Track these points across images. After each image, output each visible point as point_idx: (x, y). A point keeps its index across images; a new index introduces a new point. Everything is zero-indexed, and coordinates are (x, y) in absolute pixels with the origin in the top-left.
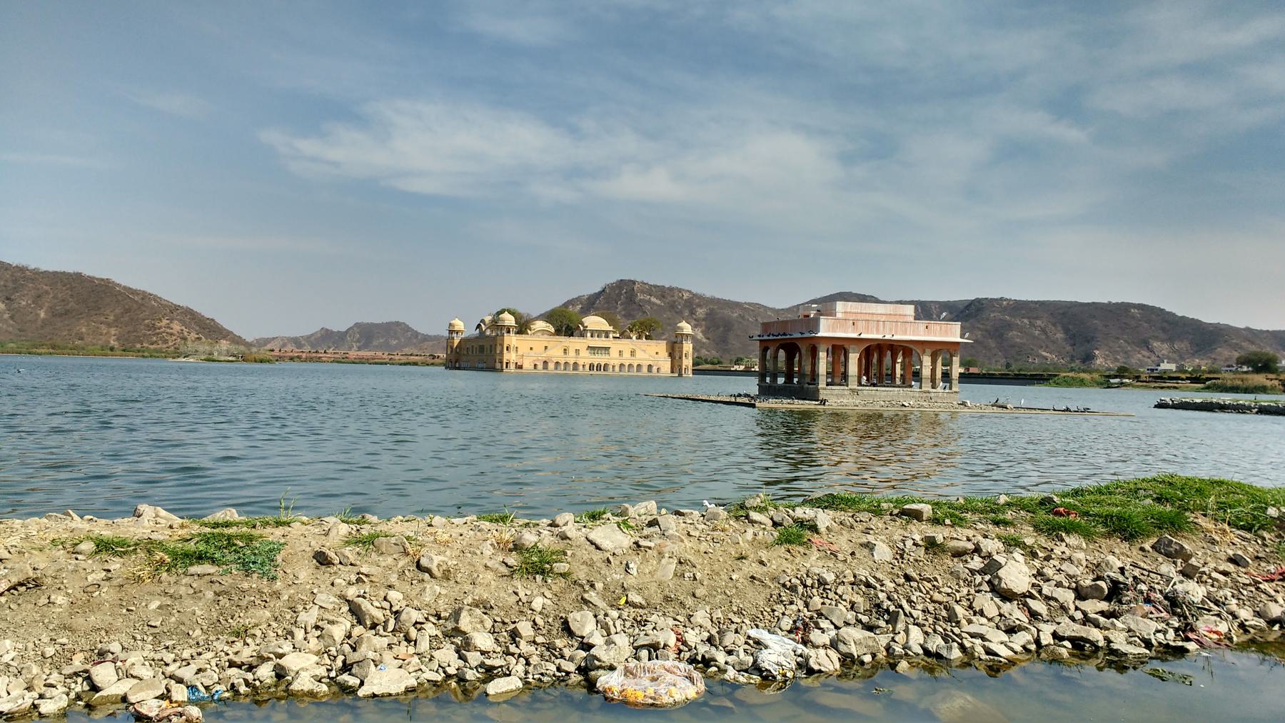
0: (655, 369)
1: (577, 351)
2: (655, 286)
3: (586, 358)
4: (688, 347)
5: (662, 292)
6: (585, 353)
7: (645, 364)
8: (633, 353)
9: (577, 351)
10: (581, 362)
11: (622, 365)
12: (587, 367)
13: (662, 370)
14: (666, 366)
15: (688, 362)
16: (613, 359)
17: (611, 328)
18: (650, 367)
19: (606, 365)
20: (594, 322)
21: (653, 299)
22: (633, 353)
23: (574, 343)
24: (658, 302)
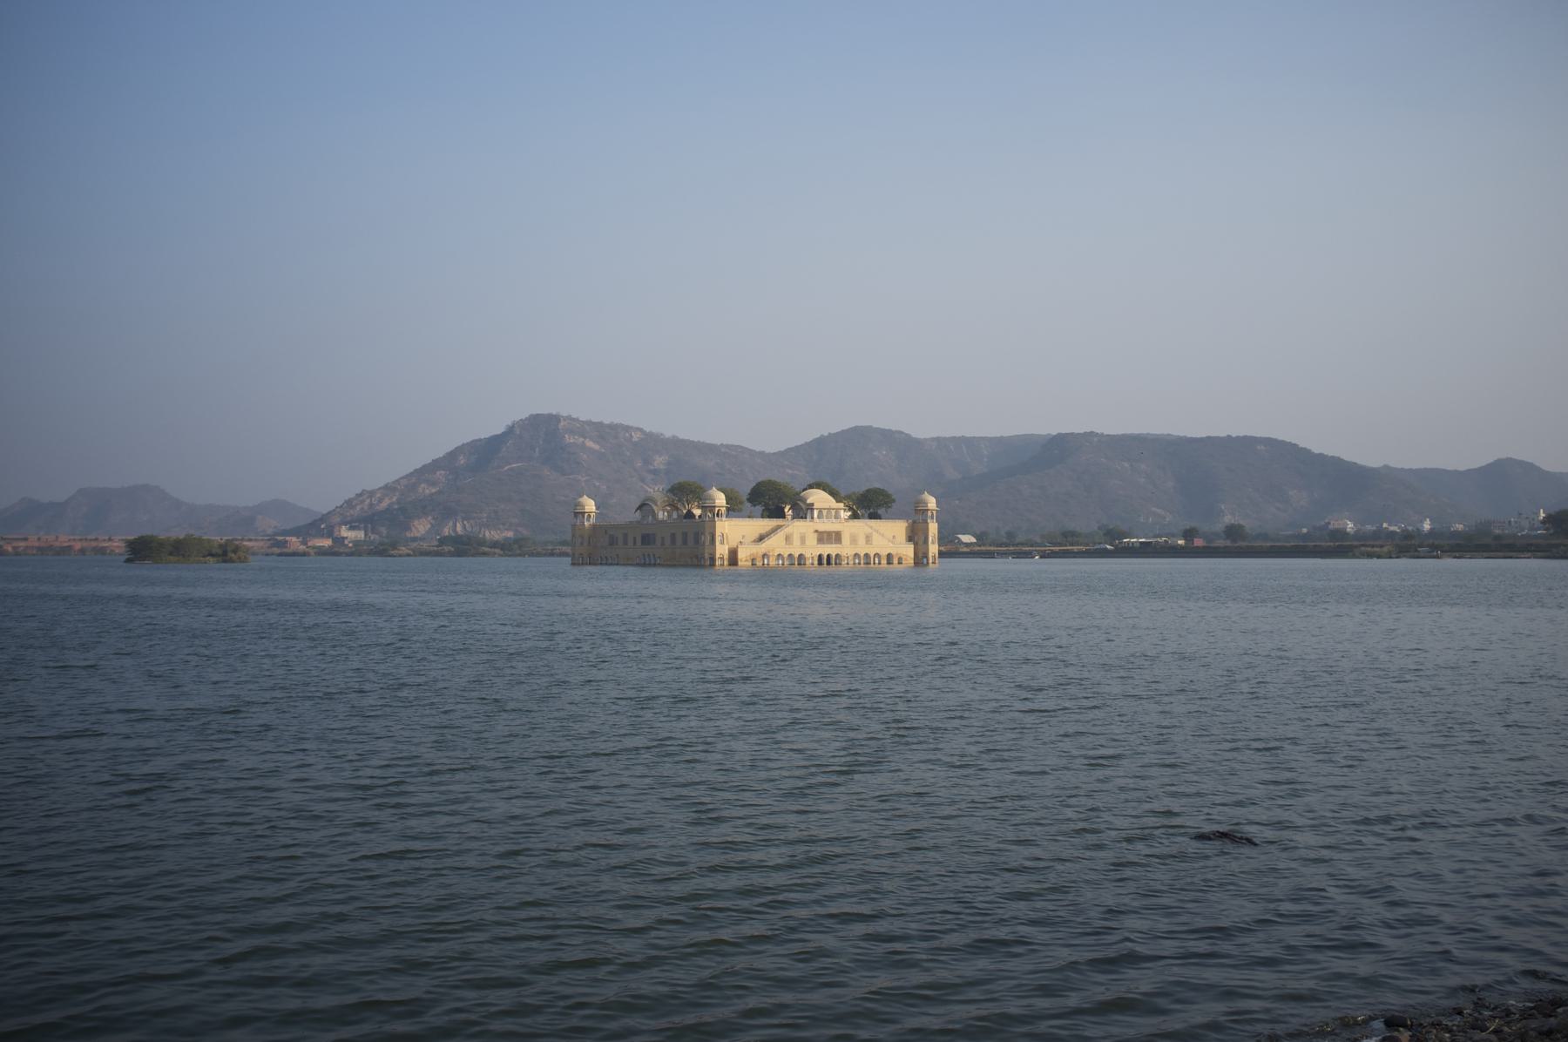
1: (803, 540)
2: (590, 423)
3: (813, 550)
4: (933, 528)
5: (601, 431)
6: (812, 539)
7: (884, 553)
8: (868, 539)
9: (803, 540)
10: (808, 555)
14: (908, 551)
15: (933, 549)
16: (845, 549)
20: (819, 498)
21: (590, 444)
22: (868, 539)
23: (797, 527)
24: (596, 447)
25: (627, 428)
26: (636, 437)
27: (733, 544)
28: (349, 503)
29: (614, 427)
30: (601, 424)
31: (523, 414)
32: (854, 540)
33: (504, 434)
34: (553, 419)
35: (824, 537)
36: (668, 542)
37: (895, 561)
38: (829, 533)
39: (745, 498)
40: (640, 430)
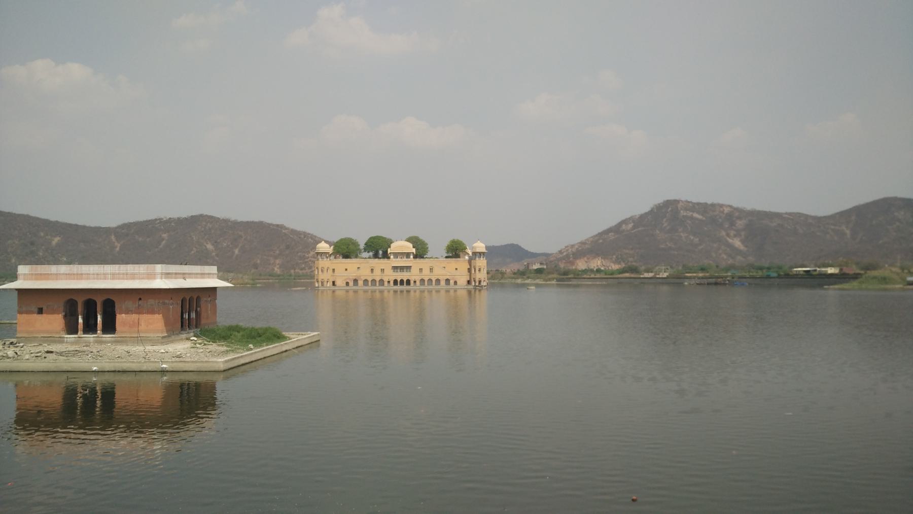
0: (452, 282)
2: (698, 204)
3: (390, 275)
8: (431, 270)
10: (386, 279)
12: (392, 283)
18: (448, 281)
22: (431, 270)
24: (700, 217)
25: (721, 206)
26: (726, 210)
28: (560, 252)
29: (713, 205)
30: (706, 204)
31: (660, 200)
32: (421, 270)
35: (395, 268)
39: (362, 246)
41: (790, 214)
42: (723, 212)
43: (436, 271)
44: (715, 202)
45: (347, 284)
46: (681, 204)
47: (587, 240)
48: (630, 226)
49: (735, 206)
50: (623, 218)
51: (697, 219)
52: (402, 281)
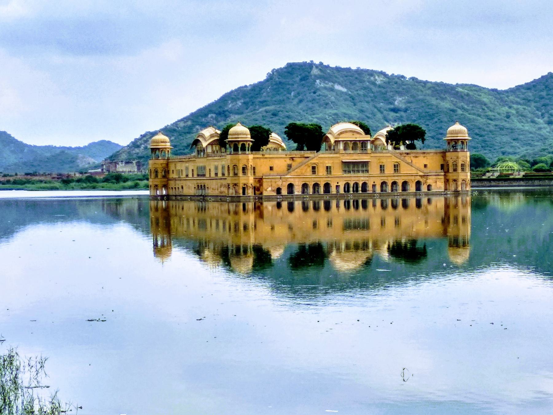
2: (338, 69)
8: (396, 167)
11: (383, 184)
13: (434, 189)
17: (368, 138)
18: (418, 184)
19: (365, 185)
21: (338, 87)
22: (396, 167)
24: (344, 90)
25: (371, 73)
26: (379, 80)
27: (259, 174)
28: (135, 144)
29: (359, 72)
30: (349, 70)
32: (382, 168)
33: (267, 80)
34: (307, 67)
35: (348, 166)
36: (213, 175)
37: (424, 188)
38: (355, 164)
40: (382, 74)
41: (463, 86)
42: (374, 83)
43: (405, 169)
44: (363, 67)
45: (279, 191)
46: (315, 71)
47: (176, 124)
48: (239, 103)
49: (390, 73)
50: (229, 91)
51: (342, 93)
52: (356, 184)
